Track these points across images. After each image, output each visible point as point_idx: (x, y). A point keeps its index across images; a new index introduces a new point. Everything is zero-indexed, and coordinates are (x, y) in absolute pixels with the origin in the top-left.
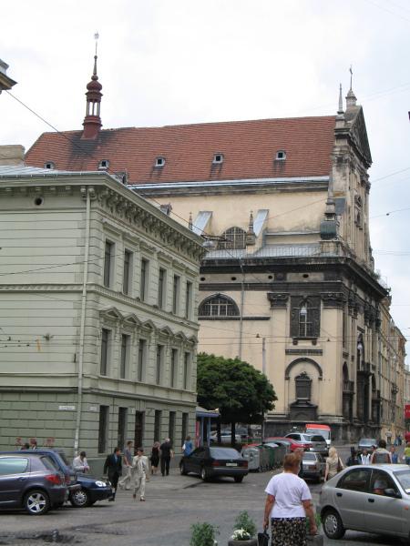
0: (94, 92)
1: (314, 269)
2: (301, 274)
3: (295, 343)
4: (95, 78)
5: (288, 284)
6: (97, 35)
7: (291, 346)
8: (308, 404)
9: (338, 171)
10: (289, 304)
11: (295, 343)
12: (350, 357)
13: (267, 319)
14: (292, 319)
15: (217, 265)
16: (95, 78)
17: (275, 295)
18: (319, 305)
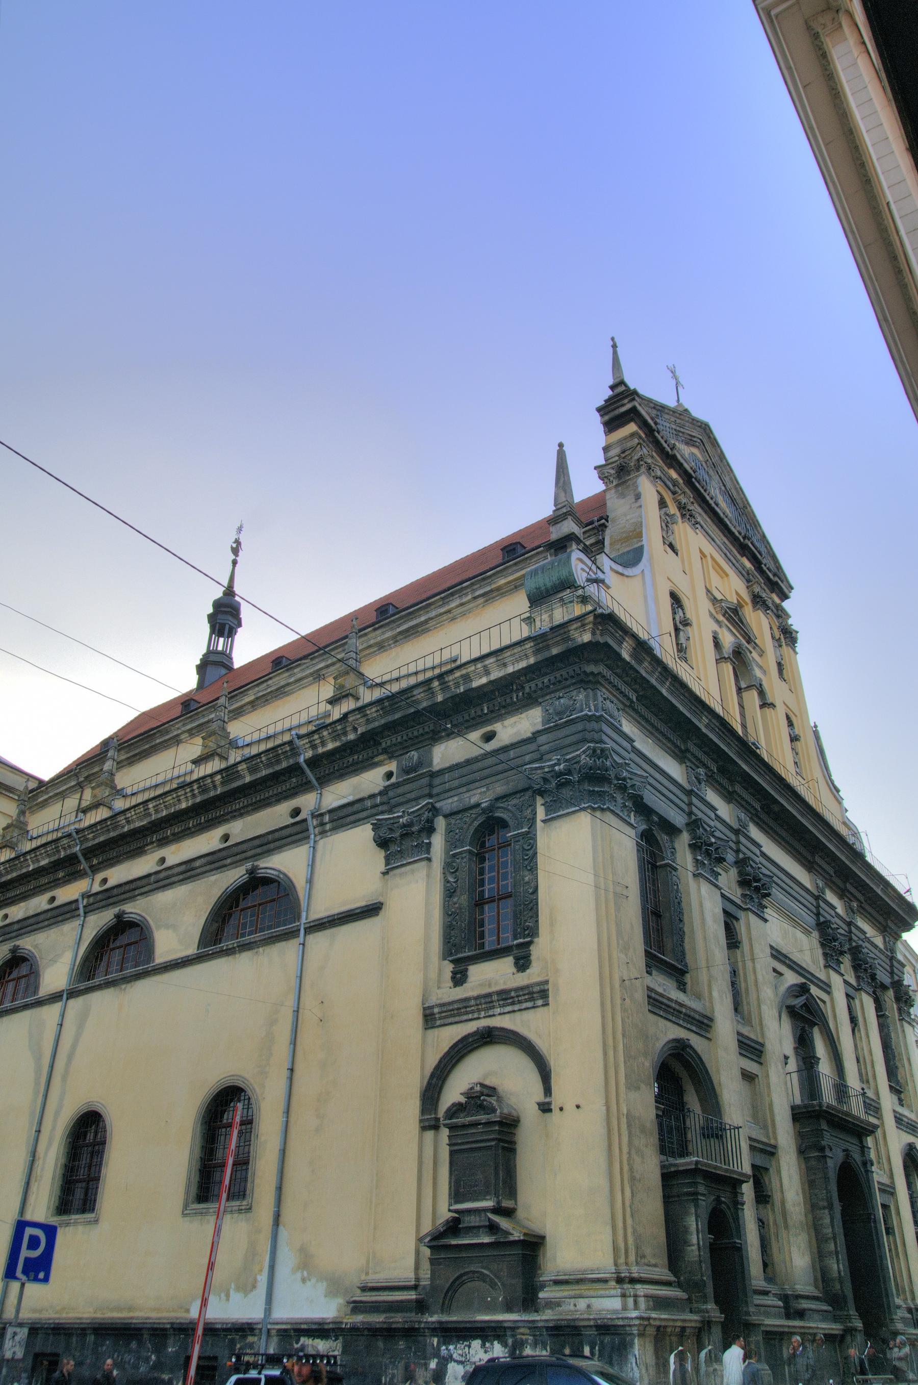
0: (225, 617)
1: (505, 696)
2: (475, 735)
3: (459, 978)
4: (230, 592)
5: (433, 775)
6: (240, 529)
7: (449, 993)
8: (493, 1228)
9: (622, 496)
10: (438, 842)
11: (459, 978)
12: (725, 1027)
13: (372, 910)
14: (449, 893)
15: (248, 779)
16: (230, 592)
17: (392, 825)
18: (532, 821)
